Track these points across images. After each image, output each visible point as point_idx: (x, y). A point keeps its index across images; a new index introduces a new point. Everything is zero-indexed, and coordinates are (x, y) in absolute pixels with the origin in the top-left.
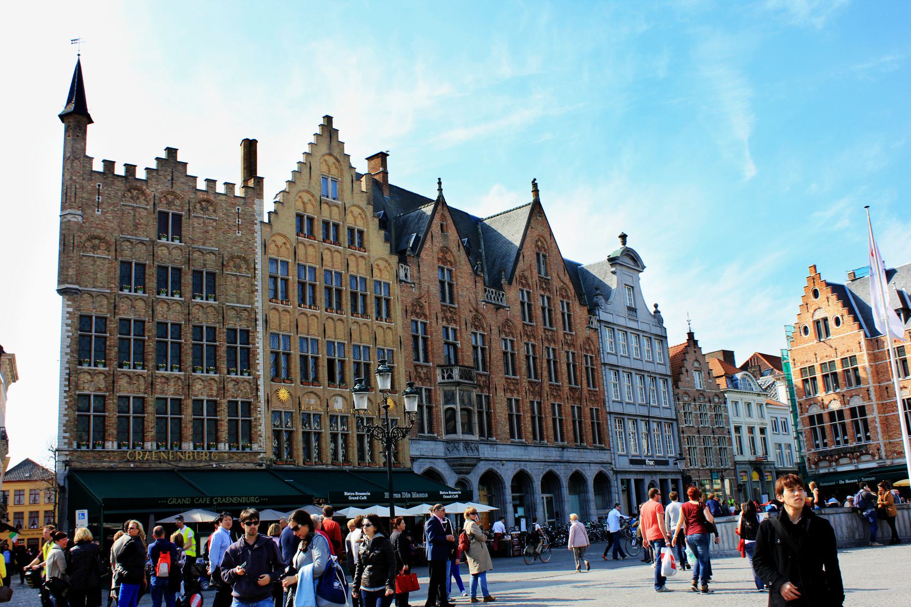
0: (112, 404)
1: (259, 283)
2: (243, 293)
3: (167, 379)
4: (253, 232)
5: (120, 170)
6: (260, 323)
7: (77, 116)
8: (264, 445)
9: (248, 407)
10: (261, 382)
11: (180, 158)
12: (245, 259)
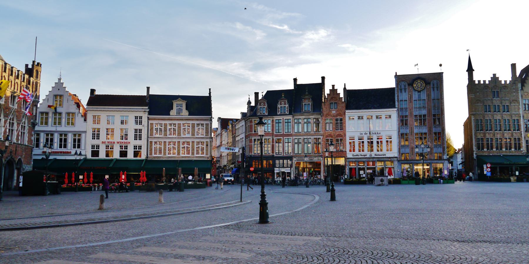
0: (485, 140)
1: (521, 107)
2: (517, 109)
3: (498, 133)
4: (518, 93)
5: (482, 82)
6: (522, 117)
7: (470, 70)
8: (524, 149)
9: (519, 139)
10: (522, 133)
11: (497, 76)
12: (516, 101)
